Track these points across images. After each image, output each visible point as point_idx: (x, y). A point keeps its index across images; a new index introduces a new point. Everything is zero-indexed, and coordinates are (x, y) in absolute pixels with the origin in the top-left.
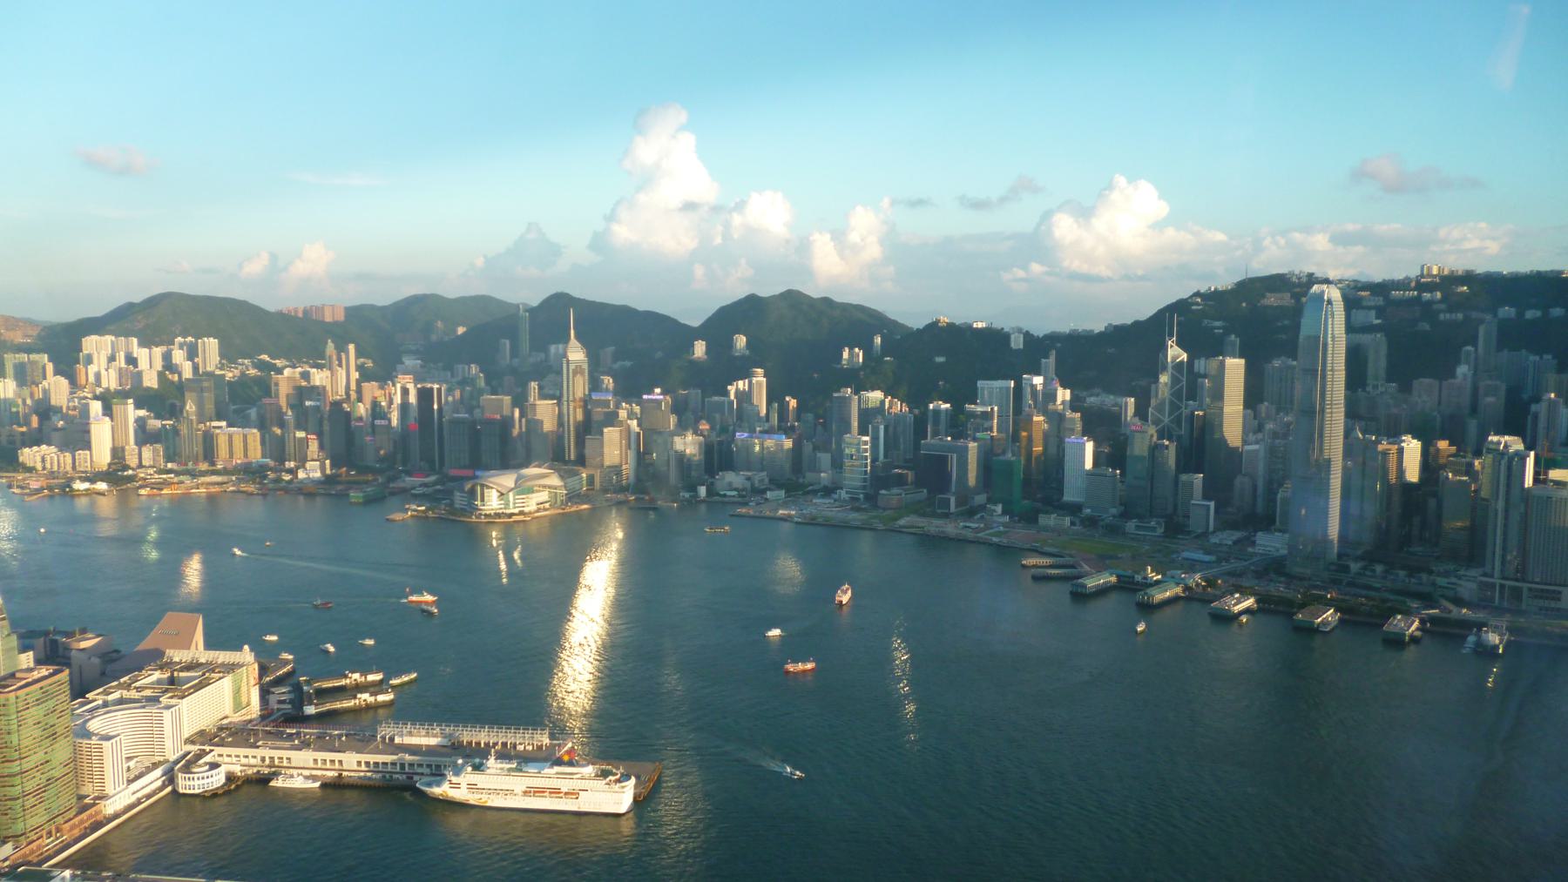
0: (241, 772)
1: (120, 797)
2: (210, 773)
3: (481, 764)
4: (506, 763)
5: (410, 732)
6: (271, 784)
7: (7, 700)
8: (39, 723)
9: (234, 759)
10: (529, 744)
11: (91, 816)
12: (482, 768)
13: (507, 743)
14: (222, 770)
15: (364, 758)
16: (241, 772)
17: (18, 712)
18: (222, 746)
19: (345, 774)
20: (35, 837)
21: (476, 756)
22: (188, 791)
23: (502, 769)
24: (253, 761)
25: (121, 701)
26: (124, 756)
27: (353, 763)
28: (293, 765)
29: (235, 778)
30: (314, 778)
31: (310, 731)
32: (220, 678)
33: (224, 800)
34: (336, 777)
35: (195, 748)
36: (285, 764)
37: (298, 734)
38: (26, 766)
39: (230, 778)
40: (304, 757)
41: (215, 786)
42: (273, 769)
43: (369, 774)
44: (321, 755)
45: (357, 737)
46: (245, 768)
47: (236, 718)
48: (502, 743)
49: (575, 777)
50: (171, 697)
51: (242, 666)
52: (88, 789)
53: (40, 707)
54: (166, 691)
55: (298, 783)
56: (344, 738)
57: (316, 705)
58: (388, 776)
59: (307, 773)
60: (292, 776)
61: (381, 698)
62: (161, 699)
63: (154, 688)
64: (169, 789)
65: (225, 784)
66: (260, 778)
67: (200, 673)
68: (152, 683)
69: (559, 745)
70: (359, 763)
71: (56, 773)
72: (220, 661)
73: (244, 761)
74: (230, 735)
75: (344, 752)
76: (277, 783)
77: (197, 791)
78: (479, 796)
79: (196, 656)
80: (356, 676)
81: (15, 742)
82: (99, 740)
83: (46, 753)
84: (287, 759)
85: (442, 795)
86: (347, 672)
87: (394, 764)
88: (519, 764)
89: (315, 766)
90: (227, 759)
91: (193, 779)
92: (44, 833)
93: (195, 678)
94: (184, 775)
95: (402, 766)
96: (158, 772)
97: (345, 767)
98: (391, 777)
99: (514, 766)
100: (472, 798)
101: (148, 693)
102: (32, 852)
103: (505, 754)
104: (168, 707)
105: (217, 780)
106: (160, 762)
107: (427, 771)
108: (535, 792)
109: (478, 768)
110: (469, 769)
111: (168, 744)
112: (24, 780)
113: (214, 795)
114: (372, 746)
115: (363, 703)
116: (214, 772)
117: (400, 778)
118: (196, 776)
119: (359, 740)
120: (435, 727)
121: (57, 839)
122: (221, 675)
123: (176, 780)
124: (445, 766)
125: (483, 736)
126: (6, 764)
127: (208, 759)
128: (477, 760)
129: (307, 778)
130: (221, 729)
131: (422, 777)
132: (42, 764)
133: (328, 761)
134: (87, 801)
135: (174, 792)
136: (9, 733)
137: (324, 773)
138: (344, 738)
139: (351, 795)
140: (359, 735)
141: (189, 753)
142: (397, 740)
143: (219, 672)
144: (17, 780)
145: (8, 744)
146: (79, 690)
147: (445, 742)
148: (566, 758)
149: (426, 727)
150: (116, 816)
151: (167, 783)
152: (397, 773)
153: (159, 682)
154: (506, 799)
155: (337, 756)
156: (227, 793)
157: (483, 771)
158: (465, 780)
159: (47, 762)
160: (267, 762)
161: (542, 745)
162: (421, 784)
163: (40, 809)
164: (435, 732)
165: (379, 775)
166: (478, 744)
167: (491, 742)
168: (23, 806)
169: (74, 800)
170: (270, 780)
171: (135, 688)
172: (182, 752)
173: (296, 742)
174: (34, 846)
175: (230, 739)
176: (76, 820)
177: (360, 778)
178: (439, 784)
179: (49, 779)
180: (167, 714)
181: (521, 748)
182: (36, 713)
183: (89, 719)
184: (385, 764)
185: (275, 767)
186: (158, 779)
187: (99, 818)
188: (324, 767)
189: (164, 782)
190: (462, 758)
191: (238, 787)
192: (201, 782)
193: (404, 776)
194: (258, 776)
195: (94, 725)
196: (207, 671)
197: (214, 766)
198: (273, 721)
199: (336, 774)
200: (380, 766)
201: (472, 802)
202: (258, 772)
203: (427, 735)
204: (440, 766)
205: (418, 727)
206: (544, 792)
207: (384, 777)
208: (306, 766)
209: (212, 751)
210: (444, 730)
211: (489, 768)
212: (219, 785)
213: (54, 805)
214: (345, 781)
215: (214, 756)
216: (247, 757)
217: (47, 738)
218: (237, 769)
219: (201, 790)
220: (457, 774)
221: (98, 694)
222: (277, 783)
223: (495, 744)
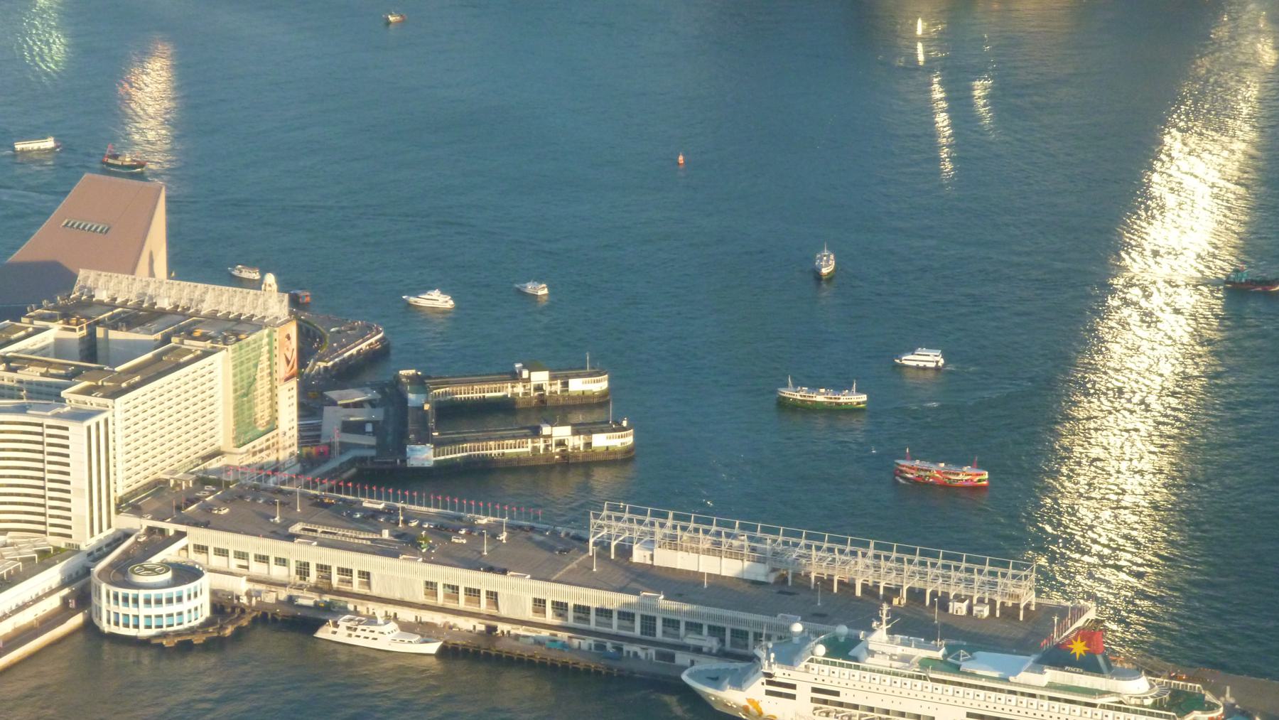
2: (174, 591)
3: (854, 641)
4: (918, 646)
5: (674, 537)
6: (321, 634)
9: (234, 563)
10: (981, 601)
13: (923, 592)
14: (206, 583)
16: (249, 594)
18: (206, 525)
19: (502, 627)
22: (122, 631)
23: (905, 659)
24: (278, 572)
28: (376, 590)
29: (234, 608)
30: (425, 631)
31: (423, 510)
32: (206, 354)
34: (481, 633)
35: (139, 524)
36: (356, 587)
37: (390, 513)
39: (222, 607)
41: (186, 625)
42: (327, 598)
43: (563, 636)
44: (444, 575)
45: (538, 537)
46: (258, 587)
47: (240, 458)
48: (910, 590)
49: (1099, 701)
50: (88, 391)
51: (259, 326)
54: (76, 374)
56: (503, 537)
57: (438, 444)
59: (408, 615)
60: (372, 620)
61: (601, 441)
62: (64, 394)
63: (49, 364)
64: (78, 619)
65: (208, 623)
66: (294, 617)
67: (158, 336)
68: (43, 350)
69: (1062, 612)
70: (539, 604)
72: (206, 309)
73: (257, 569)
74: (224, 501)
75: (504, 572)
76: (335, 633)
77: (143, 633)
79: (150, 291)
80: (541, 377)
85: (746, 709)
86: (518, 366)
87: (626, 616)
88: (951, 650)
89: (430, 601)
90: (216, 561)
91: (136, 601)
93: (143, 347)
94: (113, 589)
95: (649, 622)
96: (53, 575)
97: (504, 611)
98: (619, 649)
99: (939, 655)
101: (32, 374)
104: (80, 416)
106: (57, 549)
107: (711, 643)
109: (843, 651)
110: (821, 650)
111: (79, 506)
113: (184, 646)
114: (573, 565)
115: (555, 450)
116: (185, 589)
117: (642, 654)
118: (142, 594)
119: (541, 545)
120: (736, 531)
122: (208, 344)
123: (94, 600)
124: (758, 636)
127: (171, 554)
128: (843, 630)
129: (406, 627)
133: (462, 591)
135: (90, 627)
138: (503, 537)
139: (516, 687)
140: (541, 532)
141: (127, 535)
142: (639, 555)
143: (204, 338)
147: (761, 573)
148: (1079, 648)
149: (714, 528)
151: (72, 604)
152: (632, 640)
153: (59, 348)
155: (484, 581)
156: (215, 645)
157: (856, 659)
158: (810, 677)
160: (313, 577)
161: (1016, 606)
162: (691, 676)
164: (736, 543)
165: (587, 643)
166: (847, 586)
167: (882, 585)
170: (320, 623)
172: (107, 532)
173: (386, 534)
175: (225, 511)
177: (538, 642)
178: (738, 683)
180: (77, 431)
181: (959, 608)
184: (604, 613)
185: (330, 591)
186: (52, 592)
188: (451, 605)
189: (65, 600)
190: (804, 620)
191: (239, 632)
192: (154, 610)
193: (652, 651)
194: (289, 611)
196: (176, 333)
197: (186, 573)
198: (329, 475)
199: (481, 628)
200: (593, 616)
202: (291, 599)
203: (716, 549)
204: (744, 635)
205: (692, 525)
207: (601, 647)
208: (407, 599)
209: (180, 535)
210: (760, 540)
211: (872, 653)
212: (194, 623)
214: (503, 646)
215: (186, 548)
216: (263, 559)
218: (240, 586)
219: (153, 632)
220: (788, 659)
222: (335, 633)
223: (893, 592)
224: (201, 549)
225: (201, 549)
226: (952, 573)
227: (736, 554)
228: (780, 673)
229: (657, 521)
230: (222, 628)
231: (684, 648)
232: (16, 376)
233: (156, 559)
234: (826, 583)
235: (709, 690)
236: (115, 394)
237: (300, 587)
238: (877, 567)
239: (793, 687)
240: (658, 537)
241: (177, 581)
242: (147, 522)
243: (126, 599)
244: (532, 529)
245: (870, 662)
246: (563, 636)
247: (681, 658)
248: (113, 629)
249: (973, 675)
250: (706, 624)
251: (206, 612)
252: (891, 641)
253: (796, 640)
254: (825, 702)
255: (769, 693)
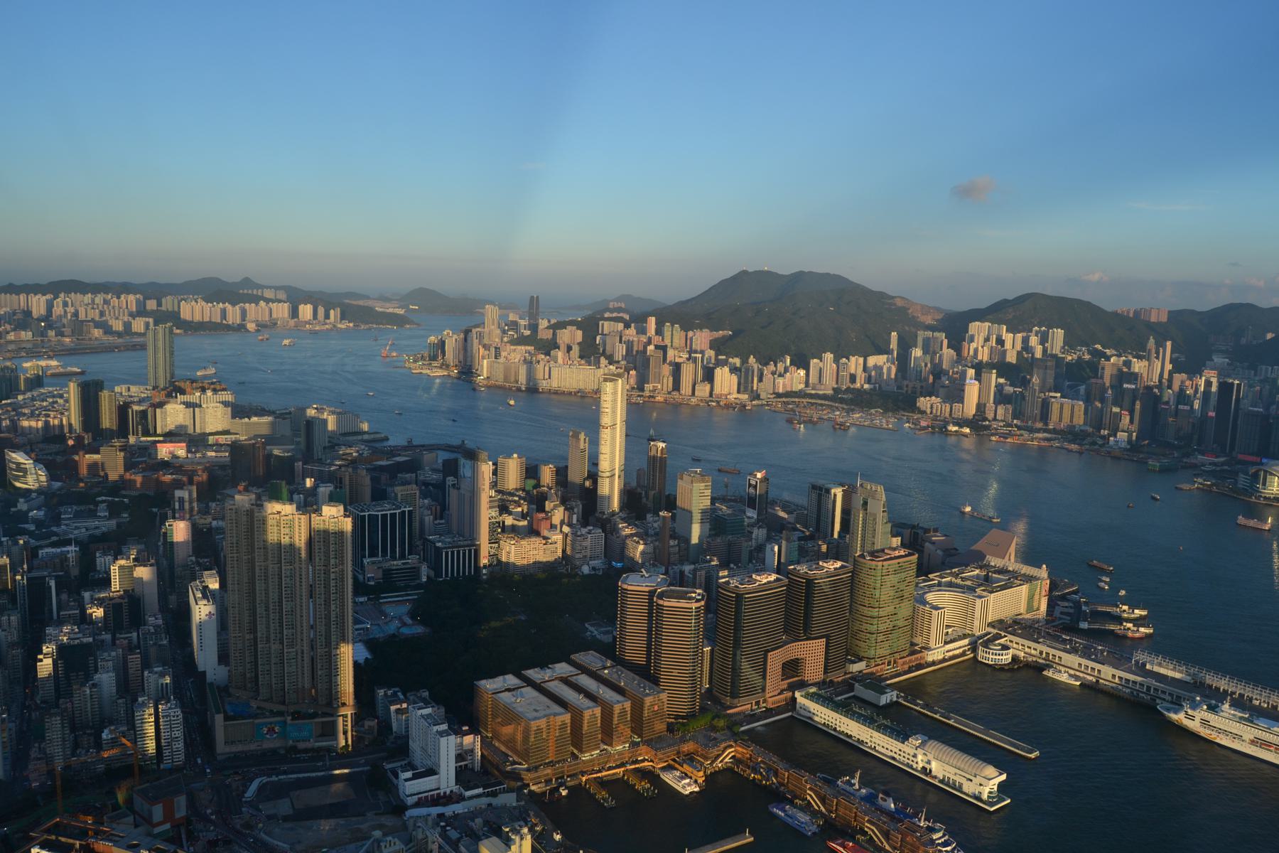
0: (1024, 657)
1: (935, 655)
4: (1239, 712)
5: (1161, 663)
6: (1045, 673)
7: (877, 566)
8: (894, 586)
9: (1020, 647)
10: (1264, 702)
11: (916, 659)
12: (1216, 710)
13: (1244, 695)
14: (1011, 651)
15: (1119, 673)
16: (1024, 657)
17: (882, 576)
18: (1014, 635)
20: (880, 663)
21: (1214, 699)
22: (984, 661)
23: (1234, 715)
25: (950, 585)
26: (945, 624)
27: (1109, 674)
28: (1062, 663)
30: (1077, 678)
33: (1009, 675)
37: (1071, 641)
38: (882, 614)
40: (1073, 660)
42: (1048, 662)
43: (1120, 687)
44: (1084, 662)
48: (1240, 694)
50: (983, 590)
52: (918, 640)
53: (896, 576)
54: (980, 585)
55: (1064, 678)
56: (1105, 654)
58: (1135, 693)
59: (1072, 672)
60: (1060, 671)
64: (972, 655)
66: (1036, 666)
70: (1114, 676)
71: (900, 623)
73: (1027, 650)
75: (1104, 664)
77: (990, 663)
78: (1209, 732)
81: (878, 596)
82: (930, 608)
83: (895, 608)
84: (1059, 657)
85: (1177, 721)
87: (1142, 685)
88: (1251, 715)
89: (1079, 669)
90: (1015, 646)
91: (989, 653)
92: (886, 661)
95: (1149, 688)
96: (966, 641)
97: (1102, 676)
98: (1138, 694)
99: (1247, 716)
100: (1204, 732)
101: (969, 583)
102: (877, 671)
103: (1240, 703)
104: (980, 597)
105: (1006, 658)
107: (1169, 698)
108: (1261, 743)
109: (1213, 709)
110: (1205, 707)
111: (976, 623)
112: (879, 622)
114: (1127, 666)
116: (1004, 652)
118: (991, 651)
121: (894, 668)
124: (1184, 699)
125: (1223, 684)
126: (870, 609)
127: (1002, 641)
128: (1214, 702)
129: (1071, 675)
130: (1015, 622)
131: (1163, 702)
132: (891, 615)
134: (916, 648)
136: (875, 589)
137: (1085, 676)
138: (1105, 654)
140: (1118, 654)
141: (990, 634)
142: (1148, 667)
144: (875, 621)
145: (873, 596)
146: (924, 570)
147: (1188, 679)
149: (1174, 663)
150: (933, 663)
154: (1233, 741)
155: (1098, 666)
156: (1011, 670)
159: (895, 614)
160: (1044, 655)
163: (886, 644)
164: (1181, 668)
165: (1128, 691)
166: (1217, 689)
167: (1230, 690)
168: (876, 639)
169: (908, 645)
170: (1044, 670)
171: (961, 578)
172: (984, 632)
174: (879, 668)
176: (908, 659)
177: (1112, 687)
178: (1176, 713)
179: (894, 627)
180: (978, 602)
182: (893, 579)
183: (927, 592)
185: (1049, 660)
186: (965, 646)
187: (923, 662)
188: (1086, 671)
191: (1019, 668)
192: (994, 657)
193: (1149, 697)
195: (930, 597)
197: (1005, 648)
201: (1202, 734)
203: (1174, 669)
204: (1180, 697)
206: (1270, 746)
207: (1132, 693)
209: (1005, 636)
210: (1190, 669)
211: (1222, 711)
213: (895, 645)
216: (1030, 648)
217: (897, 598)
219: (993, 663)
220: (1193, 708)
221: (935, 576)
222: (1049, 673)
224: (1011, 641)
225: (1011, 641)
226: (1255, 691)
227: (1180, 672)
228: (1190, 712)
229: (1156, 658)
230: (1014, 665)
231: (1160, 698)
232: (963, 583)
233: (997, 642)
234: (1210, 686)
235: (1166, 713)
236: (992, 592)
237: (1040, 658)
238: (1229, 684)
239: (1194, 717)
240: (1155, 662)
241: (1002, 649)
242: (995, 631)
243: (986, 652)
244: (1115, 653)
245: (1222, 714)
246: (1120, 687)
247: (1158, 701)
248: (982, 660)
249: (1258, 725)
250: (1168, 692)
251: (1010, 660)
252: (1230, 709)
253: (1197, 702)
254: (1205, 724)
255: (1186, 717)
